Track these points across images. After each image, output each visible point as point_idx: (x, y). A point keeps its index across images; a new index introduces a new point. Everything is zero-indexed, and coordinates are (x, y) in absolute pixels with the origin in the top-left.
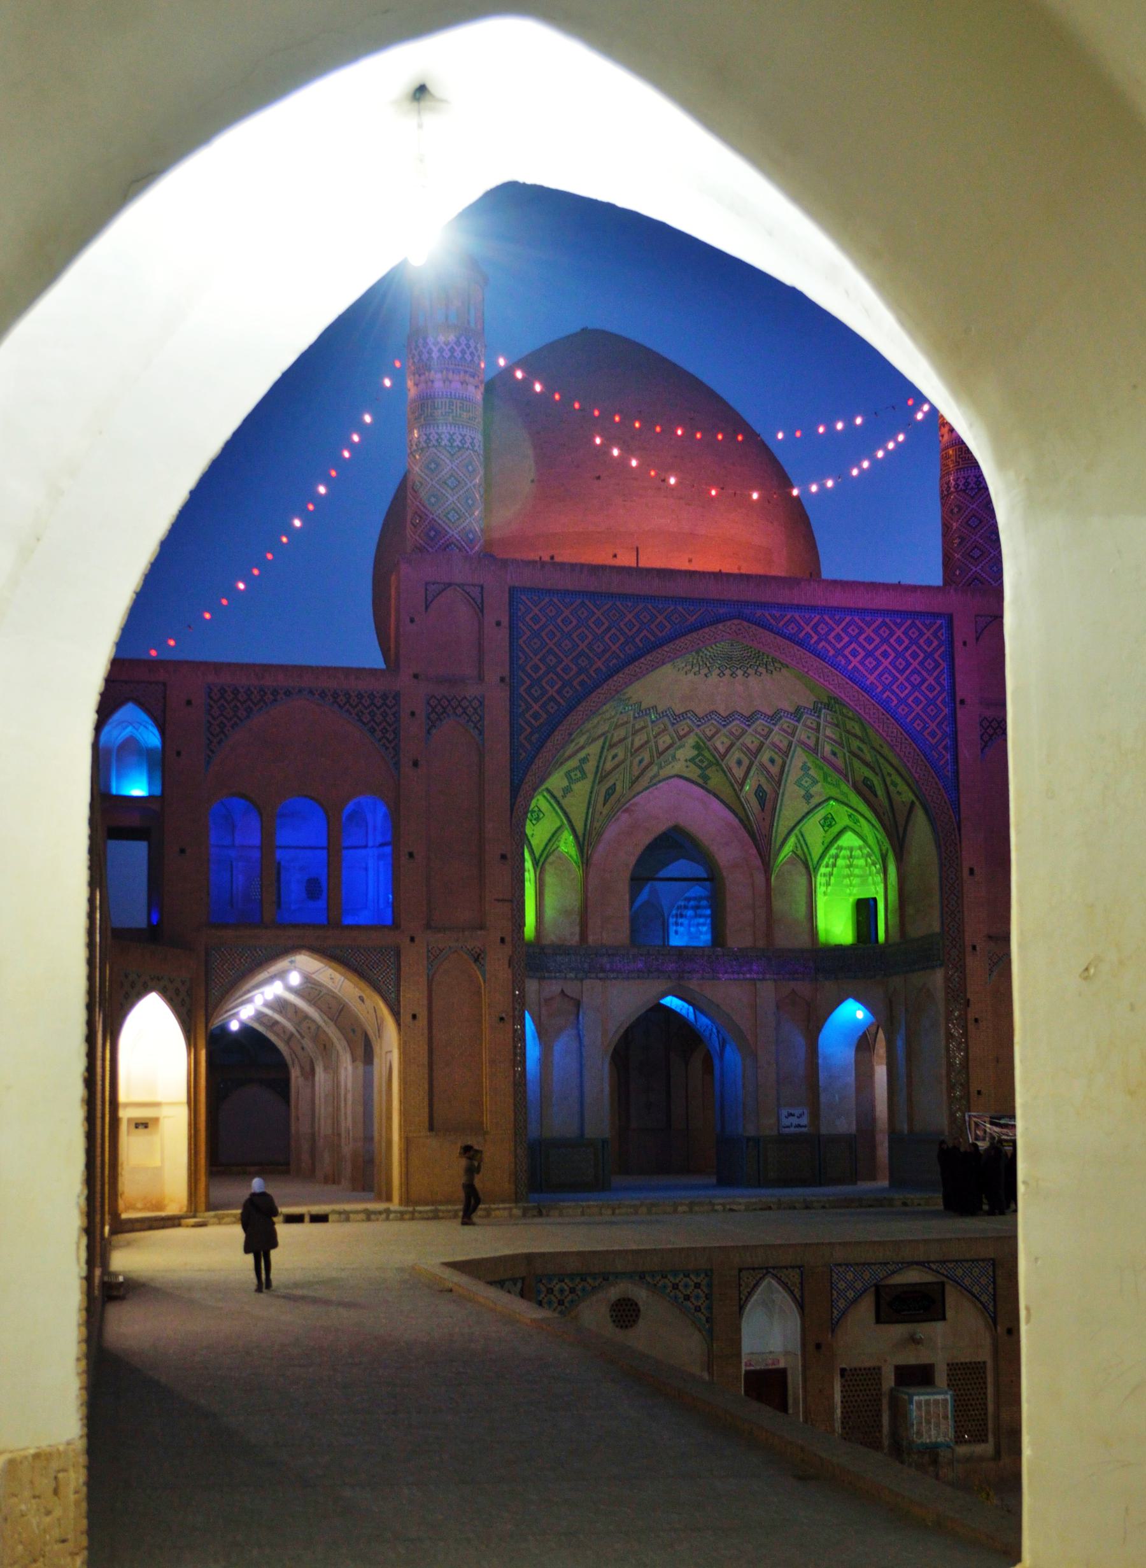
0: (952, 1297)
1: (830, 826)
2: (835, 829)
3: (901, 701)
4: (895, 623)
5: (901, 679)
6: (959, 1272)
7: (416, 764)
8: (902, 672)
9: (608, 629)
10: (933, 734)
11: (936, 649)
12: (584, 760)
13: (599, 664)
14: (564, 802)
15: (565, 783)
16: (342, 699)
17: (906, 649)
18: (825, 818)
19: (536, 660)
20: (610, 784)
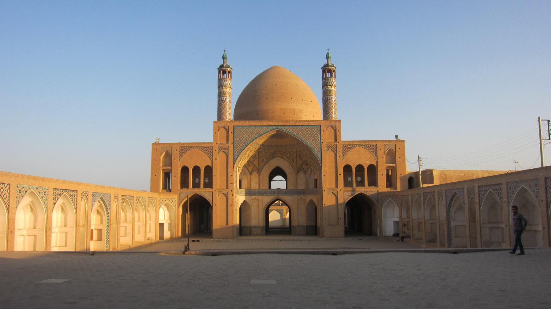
3: (310, 143)
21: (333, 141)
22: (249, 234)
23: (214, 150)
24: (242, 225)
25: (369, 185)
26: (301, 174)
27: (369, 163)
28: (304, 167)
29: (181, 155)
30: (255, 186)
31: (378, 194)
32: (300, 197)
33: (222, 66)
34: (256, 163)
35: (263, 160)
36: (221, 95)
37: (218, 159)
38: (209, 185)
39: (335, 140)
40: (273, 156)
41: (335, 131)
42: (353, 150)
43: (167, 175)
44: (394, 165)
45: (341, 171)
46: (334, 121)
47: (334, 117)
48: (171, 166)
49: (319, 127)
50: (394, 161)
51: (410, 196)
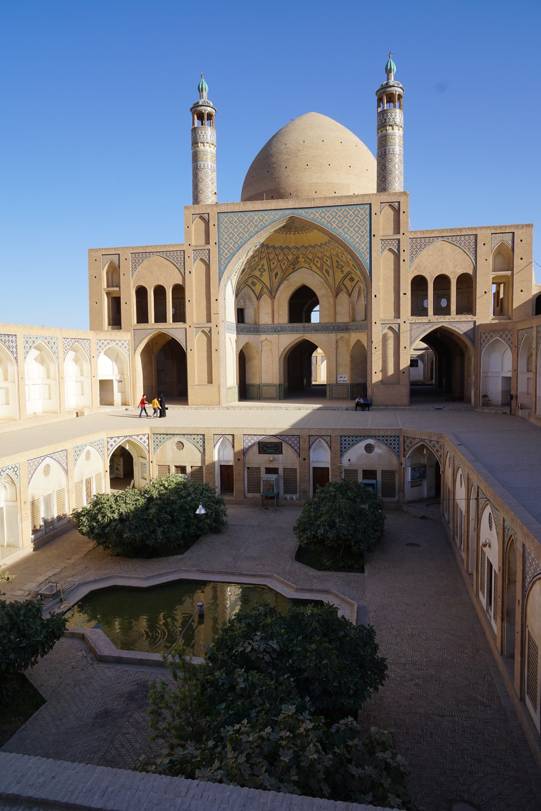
0: (285, 446)
1: (353, 281)
2: (355, 282)
3: (351, 237)
4: (349, 209)
5: (351, 229)
6: (287, 439)
7: (190, 272)
8: (351, 227)
9: (249, 223)
10: (363, 248)
11: (365, 217)
12: (263, 265)
13: (246, 235)
14: (261, 279)
15: (260, 273)
16: (168, 254)
17: (354, 218)
18: (351, 278)
19: (226, 236)
20: (275, 272)
21: (391, 232)
22: (259, 398)
23: (186, 257)
24: (248, 382)
25: (459, 312)
26: (343, 297)
27: (460, 272)
28: (347, 282)
29: (134, 268)
30: (265, 319)
31: (476, 328)
32: (340, 335)
33: (197, 105)
34: (265, 278)
35: (276, 275)
36: (196, 157)
37: (193, 272)
38: (180, 316)
39: (397, 229)
40: (294, 266)
41: (397, 212)
42: (431, 247)
43: (116, 303)
44: (509, 273)
45: (406, 287)
46: (395, 194)
47: (397, 184)
48: (118, 286)
49: (368, 206)
50: (511, 268)
51: (535, 329)
